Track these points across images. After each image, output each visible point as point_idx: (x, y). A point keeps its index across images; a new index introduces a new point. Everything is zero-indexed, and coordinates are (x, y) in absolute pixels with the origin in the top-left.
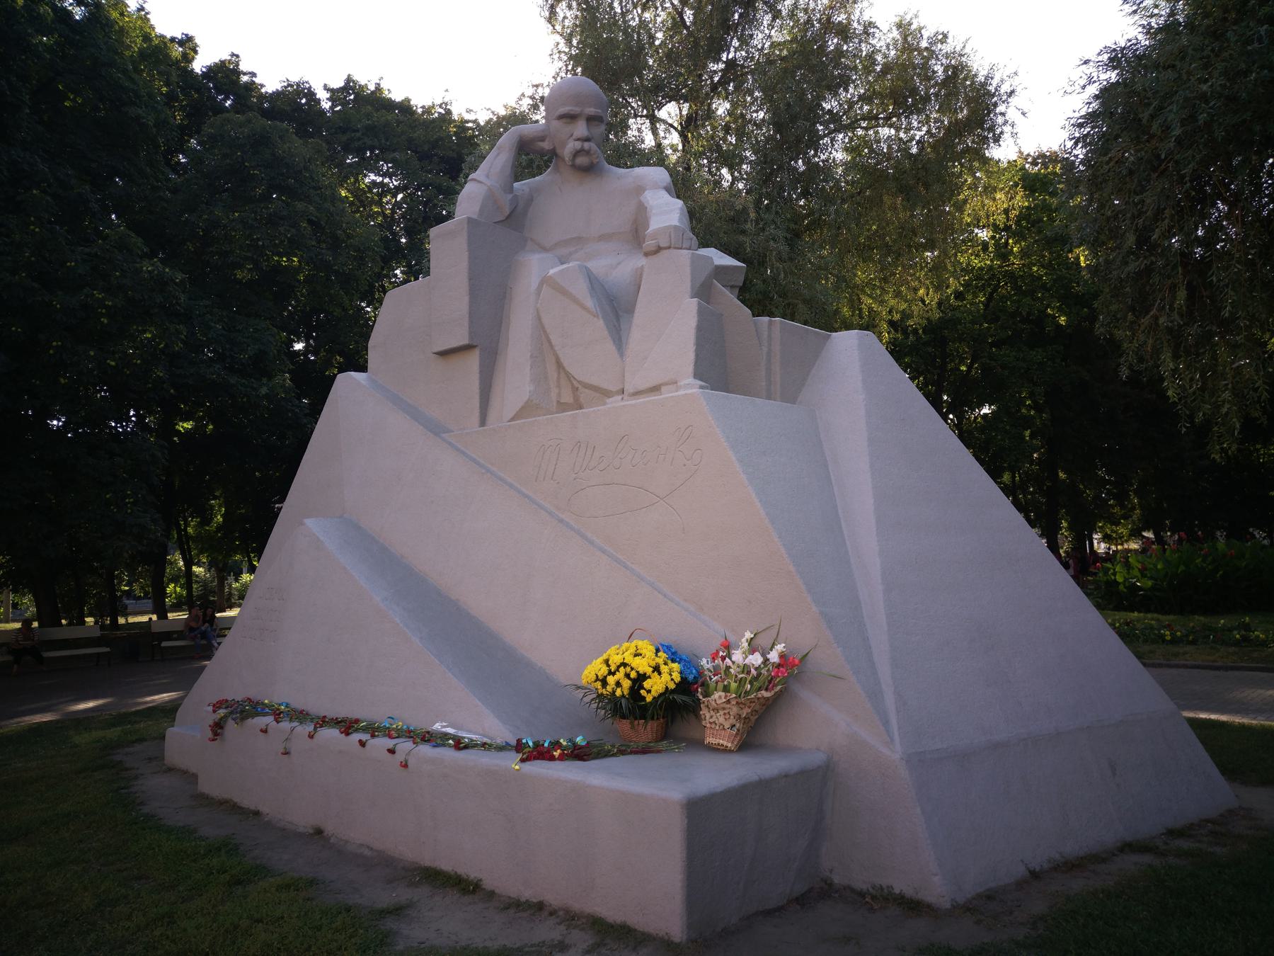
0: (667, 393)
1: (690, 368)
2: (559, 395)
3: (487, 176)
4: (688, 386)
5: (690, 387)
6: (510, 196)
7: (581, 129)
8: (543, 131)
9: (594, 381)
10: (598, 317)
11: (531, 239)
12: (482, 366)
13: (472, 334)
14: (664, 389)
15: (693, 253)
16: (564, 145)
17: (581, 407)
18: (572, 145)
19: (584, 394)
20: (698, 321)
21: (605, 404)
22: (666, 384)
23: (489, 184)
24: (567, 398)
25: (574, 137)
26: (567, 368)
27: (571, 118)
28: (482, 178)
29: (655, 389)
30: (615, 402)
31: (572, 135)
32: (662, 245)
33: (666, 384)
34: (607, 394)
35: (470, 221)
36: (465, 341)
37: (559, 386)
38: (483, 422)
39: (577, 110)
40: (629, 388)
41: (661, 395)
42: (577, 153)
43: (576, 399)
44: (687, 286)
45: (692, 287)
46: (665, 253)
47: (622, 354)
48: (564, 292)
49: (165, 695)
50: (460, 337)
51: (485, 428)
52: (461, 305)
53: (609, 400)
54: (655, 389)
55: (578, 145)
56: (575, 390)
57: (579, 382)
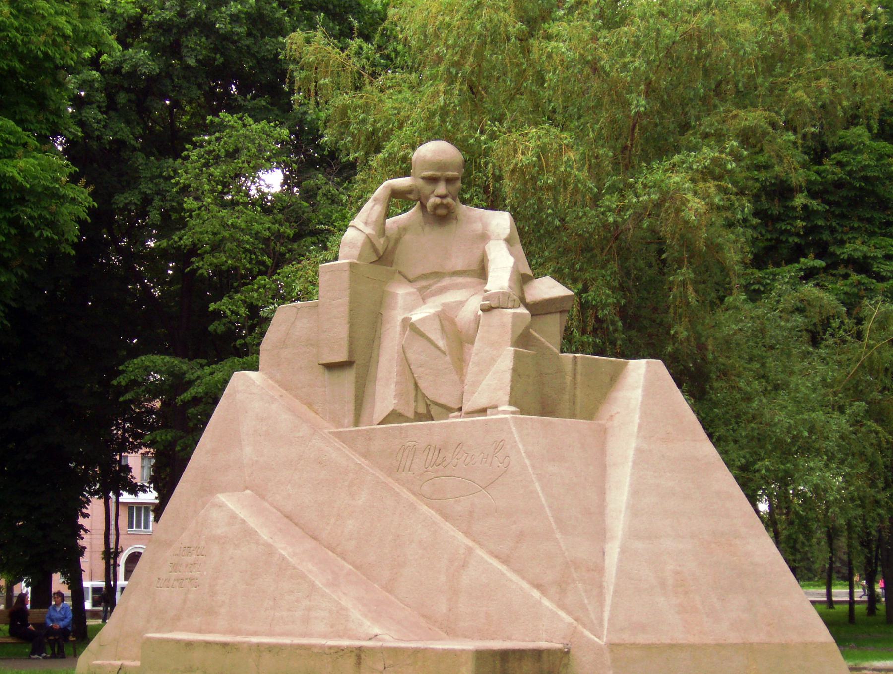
1: (507, 398)
2: (416, 407)
3: (366, 223)
4: (504, 412)
5: (506, 410)
6: (382, 240)
7: (441, 188)
9: (442, 401)
10: (444, 353)
11: (400, 273)
12: (357, 378)
13: (351, 352)
14: (489, 411)
15: (514, 314)
16: (427, 198)
18: (433, 200)
19: (434, 410)
20: (514, 364)
21: (448, 418)
24: (422, 410)
25: (435, 193)
27: (433, 180)
28: (361, 226)
29: (483, 411)
30: (454, 419)
32: (493, 306)
34: (450, 410)
35: (352, 265)
36: (342, 357)
37: (416, 401)
38: (357, 423)
39: (438, 174)
41: (486, 416)
42: (436, 207)
43: (429, 411)
44: (508, 337)
45: (512, 339)
46: (496, 312)
47: (463, 382)
48: (422, 335)
49: (93, 623)
52: (341, 331)
54: (483, 411)
55: (438, 200)
56: (428, 406)
57: (431, 401)
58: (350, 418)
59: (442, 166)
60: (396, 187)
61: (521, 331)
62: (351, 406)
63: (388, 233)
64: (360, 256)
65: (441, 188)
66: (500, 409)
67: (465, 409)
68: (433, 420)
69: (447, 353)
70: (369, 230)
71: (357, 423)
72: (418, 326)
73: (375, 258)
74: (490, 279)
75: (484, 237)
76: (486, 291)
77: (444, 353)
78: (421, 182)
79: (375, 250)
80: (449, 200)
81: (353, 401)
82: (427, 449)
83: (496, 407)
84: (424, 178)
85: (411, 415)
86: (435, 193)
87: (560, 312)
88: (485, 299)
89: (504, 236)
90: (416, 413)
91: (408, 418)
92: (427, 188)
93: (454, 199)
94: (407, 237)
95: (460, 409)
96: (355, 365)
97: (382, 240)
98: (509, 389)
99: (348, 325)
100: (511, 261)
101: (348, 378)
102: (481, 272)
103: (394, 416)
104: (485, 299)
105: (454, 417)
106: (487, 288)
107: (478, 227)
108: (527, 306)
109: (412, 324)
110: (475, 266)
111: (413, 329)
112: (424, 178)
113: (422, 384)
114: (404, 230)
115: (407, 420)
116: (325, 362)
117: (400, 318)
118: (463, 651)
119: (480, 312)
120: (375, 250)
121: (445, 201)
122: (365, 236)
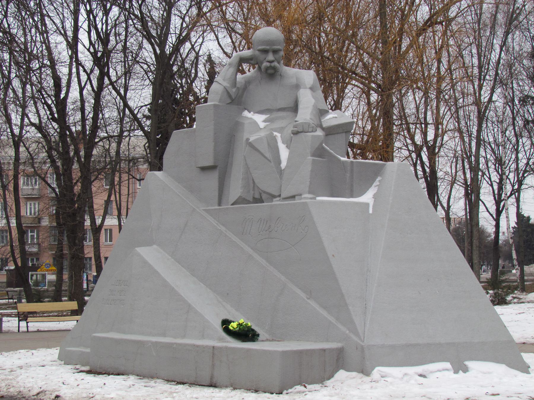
0: (297, 201)
1: (307, 189)
2: (254, 194)
3: (224, 80)
4: (305, 198)
6: (234, 90)
7: (271, 57)
8: (251, 56)
10: (270, 161)
14: (297, 197)
16: (262, 63)
17: (262, 202)
18: (265, 64)
21: (272, 201)
22: (297, 195)
23: (224, 85)
24: (257, 196)
26: (257, 184)
29: (293, 197)
30: (276, 202)
31: (265, 59)
33: (297, 195)
34: (274, 197)
35: (215, 106)
38: (220, 204)
39: (268, 47)
40: (283, 196)
41: (295, 200)
42: (267, 69)
47: (281, 179)
48: (257, 150)
50: (209, 162)
51: (221, 207)
53: (274, 200)
54: (293, 197)
55: (268, 64)
56: (260, 194)
57: (262, 191)
58: (216, 200)
59: (271, 42)
60: (242, 56)
61: (317, 146)
62: (216, 193)
63: (238, 85)
64: (220, 101)
65: (271, 57)
66: (303, 196)
67: (283, 196)
68: (263, 202)
69: (272, 161)
70: (226, 84)
71: (220, 204)
72: (254, 144)
73: (229, 101)
74: (299, 113)
75: (297, 87)
76: (296, 121)
77: (270, 161)
78: (257, 53)
79: (229, 96)
80: (276, 64)
81: (217, 190)
82: (260, 221)
83: (301, 195)
84: (259, 50)
85: (251, 199)
86: (267, 59)
87: (346, 132)
88: (295, 127)
89: (309, 86)
90: (254, 198)
91: (249, 201)
92: (261, 56)
93: (279, 63)
94: (251, 87)
95: (280, 196)
96: (218, 168)
97: (234, 90)
98: (308, 183)
99: (213, 143)
100: (313, 101)
101: (214, 176)
102: (295, 108)
103: (240, 201)
104: (295, 127)
105: (276, 201)
106: (296, 119)
107: (294, 81)
108: (323, 129)
109: (250, 143)
110: (292, 105)
111: (251, 145)
112: (259, 50)
113: (256, 181)
114: (248, 83)
115: (249, 202)
116: (200, 166)
117: (245, 139)
118: (275, 351)
119: (292, 135)
120: (229, 96)
121: (273, 64)
122: (223, 87)
